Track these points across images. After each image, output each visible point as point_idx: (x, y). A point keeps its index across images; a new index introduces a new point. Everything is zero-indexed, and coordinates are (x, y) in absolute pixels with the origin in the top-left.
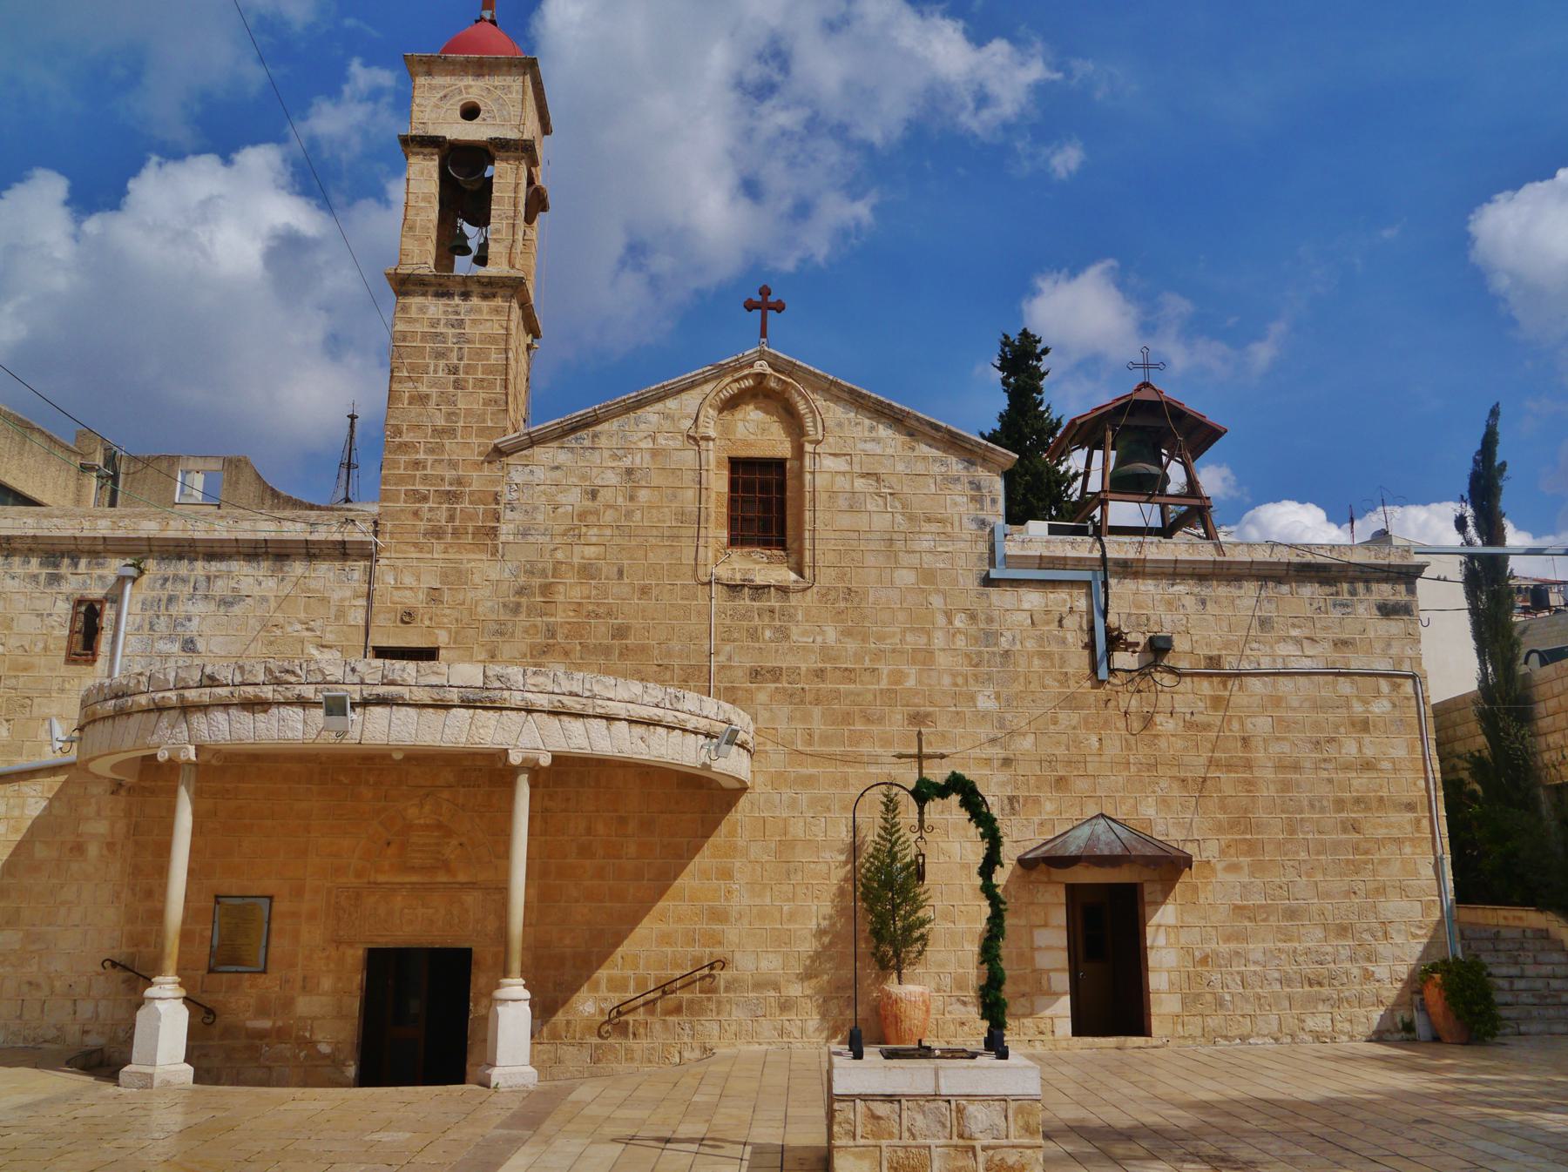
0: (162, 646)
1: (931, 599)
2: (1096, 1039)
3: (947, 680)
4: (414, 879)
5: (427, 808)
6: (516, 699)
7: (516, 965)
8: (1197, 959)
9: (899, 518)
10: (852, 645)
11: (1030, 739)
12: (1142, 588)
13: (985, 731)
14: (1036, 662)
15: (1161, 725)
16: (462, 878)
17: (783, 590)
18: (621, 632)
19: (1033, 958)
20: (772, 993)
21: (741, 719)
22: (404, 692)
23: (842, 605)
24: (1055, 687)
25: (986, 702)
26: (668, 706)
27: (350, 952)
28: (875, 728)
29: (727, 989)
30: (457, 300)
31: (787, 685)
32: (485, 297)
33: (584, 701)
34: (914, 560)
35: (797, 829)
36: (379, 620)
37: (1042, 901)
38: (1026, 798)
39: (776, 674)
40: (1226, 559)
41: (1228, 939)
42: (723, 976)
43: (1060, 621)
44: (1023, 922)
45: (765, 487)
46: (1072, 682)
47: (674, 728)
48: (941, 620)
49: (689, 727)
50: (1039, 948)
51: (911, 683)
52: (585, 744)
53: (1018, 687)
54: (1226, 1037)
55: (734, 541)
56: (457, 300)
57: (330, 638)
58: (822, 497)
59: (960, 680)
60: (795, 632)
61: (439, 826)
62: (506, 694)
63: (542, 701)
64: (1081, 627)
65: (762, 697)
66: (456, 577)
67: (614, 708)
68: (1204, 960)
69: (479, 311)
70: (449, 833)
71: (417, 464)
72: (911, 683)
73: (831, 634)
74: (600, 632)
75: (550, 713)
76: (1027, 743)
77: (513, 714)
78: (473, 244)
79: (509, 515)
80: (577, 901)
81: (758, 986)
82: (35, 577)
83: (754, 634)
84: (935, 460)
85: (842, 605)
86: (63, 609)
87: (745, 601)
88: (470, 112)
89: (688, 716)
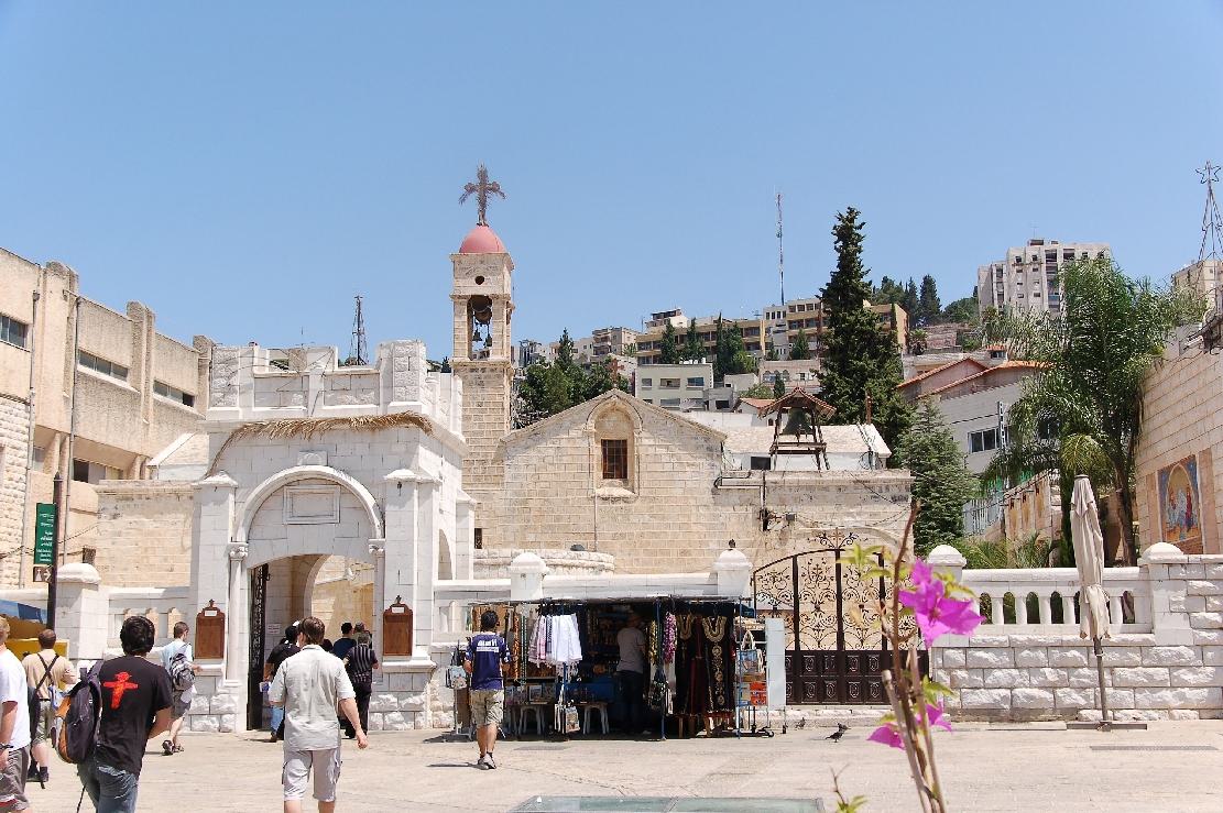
17: (625, 499)
21: (605, 557)
32: (492, 370)
39: (623, 536)
45: (618, 451)
48: (694, 511)
51: (681, 538)
66: (486, 495)
69: (490, 377)
72: (681, 538)
73: (647, 517)
78: (484, 337)
83: (614, 519)
87: (608, 505)
88: (480, 280)
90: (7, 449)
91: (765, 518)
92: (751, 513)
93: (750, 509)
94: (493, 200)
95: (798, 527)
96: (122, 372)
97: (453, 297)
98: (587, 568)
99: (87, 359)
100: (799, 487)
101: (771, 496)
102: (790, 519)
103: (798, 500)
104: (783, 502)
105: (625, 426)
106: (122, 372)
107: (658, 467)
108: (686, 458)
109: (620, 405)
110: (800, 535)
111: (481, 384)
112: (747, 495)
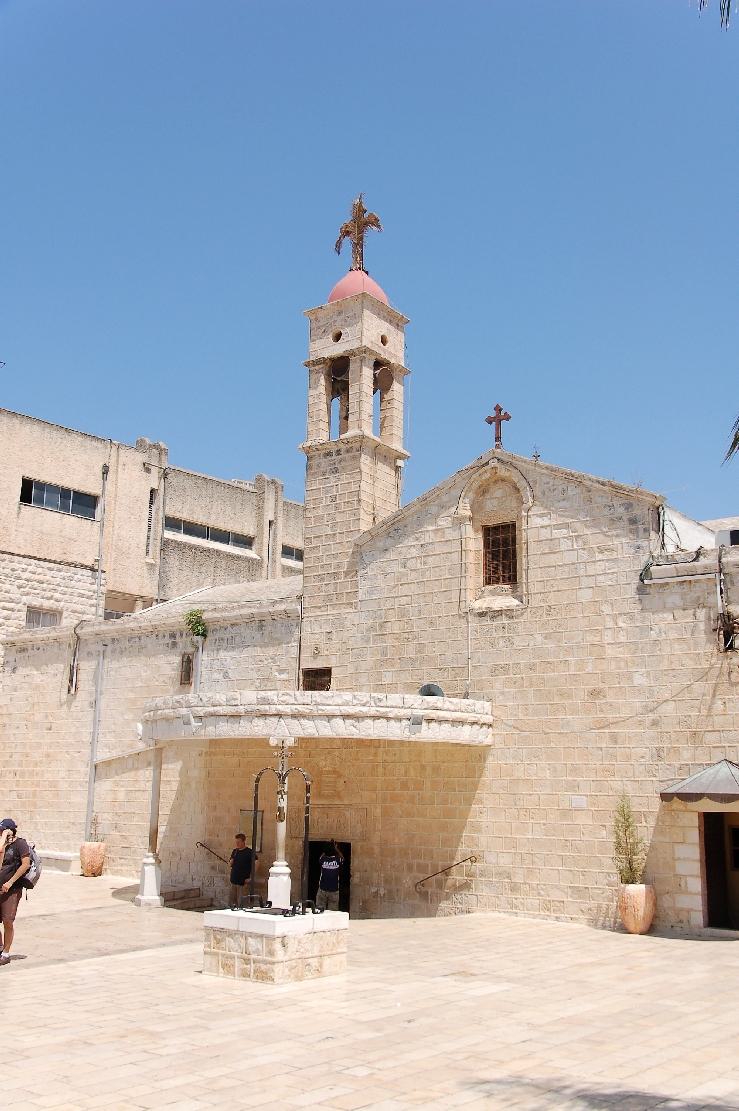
0: (216, 676)
1: (603, 608)
2: (727, 931)
3: (613, 665)
6: (273, 709)
7: (281, 854)
10: (550, 645)
11: (672, 705)
13: (638, 702)
14: (676, 646)
16: (346, 802)
17: (508, 613)
18: (421, 648)
19: (674, 867)
22: (220, 710)
23: (545, 618)
24: (690, 664)
25: (638, 680)
26: (373, 704)
28: (567, 702)
29: (482, 875)
31: (512, 676)
32: (348, 451)
34: (590, 582)
37: (681, 824)
38: (669, 749)
39: (505, 669)
45: (505, 542)
46: (703, 661)
47: (379, 718)
48: (610, 624)
49: (391, 715)
50: (679, 859)
51: (589, 669)
52: (314, 731)
53: (665, 665)
55: (488, 582)
57: (283, 666)
58: (532, 546)
59: (622, 664)
60: (517, 641)
61: (335, 772)
62: (267, 707)
63: (287, 709)
64: (709, 619)
67: (329, 710)
70: (340, 776)
73: (539, 638)
74: (410, 651)
76: (669, 708)
77: (273, 719)
81: (500, 874)
85: (545, 618)
86: (177, 660)
87: (487, 621)
88: (338, 337)
89: (388, 710)
90: (65, 614)
93: (702, 614)
94: (371, 233)
96: (246, 542)
97: (307, 365)
98: (399, 719)
106: (246, 542)
107: (553, 559)
108: (594, 537)
109: (503, 472)
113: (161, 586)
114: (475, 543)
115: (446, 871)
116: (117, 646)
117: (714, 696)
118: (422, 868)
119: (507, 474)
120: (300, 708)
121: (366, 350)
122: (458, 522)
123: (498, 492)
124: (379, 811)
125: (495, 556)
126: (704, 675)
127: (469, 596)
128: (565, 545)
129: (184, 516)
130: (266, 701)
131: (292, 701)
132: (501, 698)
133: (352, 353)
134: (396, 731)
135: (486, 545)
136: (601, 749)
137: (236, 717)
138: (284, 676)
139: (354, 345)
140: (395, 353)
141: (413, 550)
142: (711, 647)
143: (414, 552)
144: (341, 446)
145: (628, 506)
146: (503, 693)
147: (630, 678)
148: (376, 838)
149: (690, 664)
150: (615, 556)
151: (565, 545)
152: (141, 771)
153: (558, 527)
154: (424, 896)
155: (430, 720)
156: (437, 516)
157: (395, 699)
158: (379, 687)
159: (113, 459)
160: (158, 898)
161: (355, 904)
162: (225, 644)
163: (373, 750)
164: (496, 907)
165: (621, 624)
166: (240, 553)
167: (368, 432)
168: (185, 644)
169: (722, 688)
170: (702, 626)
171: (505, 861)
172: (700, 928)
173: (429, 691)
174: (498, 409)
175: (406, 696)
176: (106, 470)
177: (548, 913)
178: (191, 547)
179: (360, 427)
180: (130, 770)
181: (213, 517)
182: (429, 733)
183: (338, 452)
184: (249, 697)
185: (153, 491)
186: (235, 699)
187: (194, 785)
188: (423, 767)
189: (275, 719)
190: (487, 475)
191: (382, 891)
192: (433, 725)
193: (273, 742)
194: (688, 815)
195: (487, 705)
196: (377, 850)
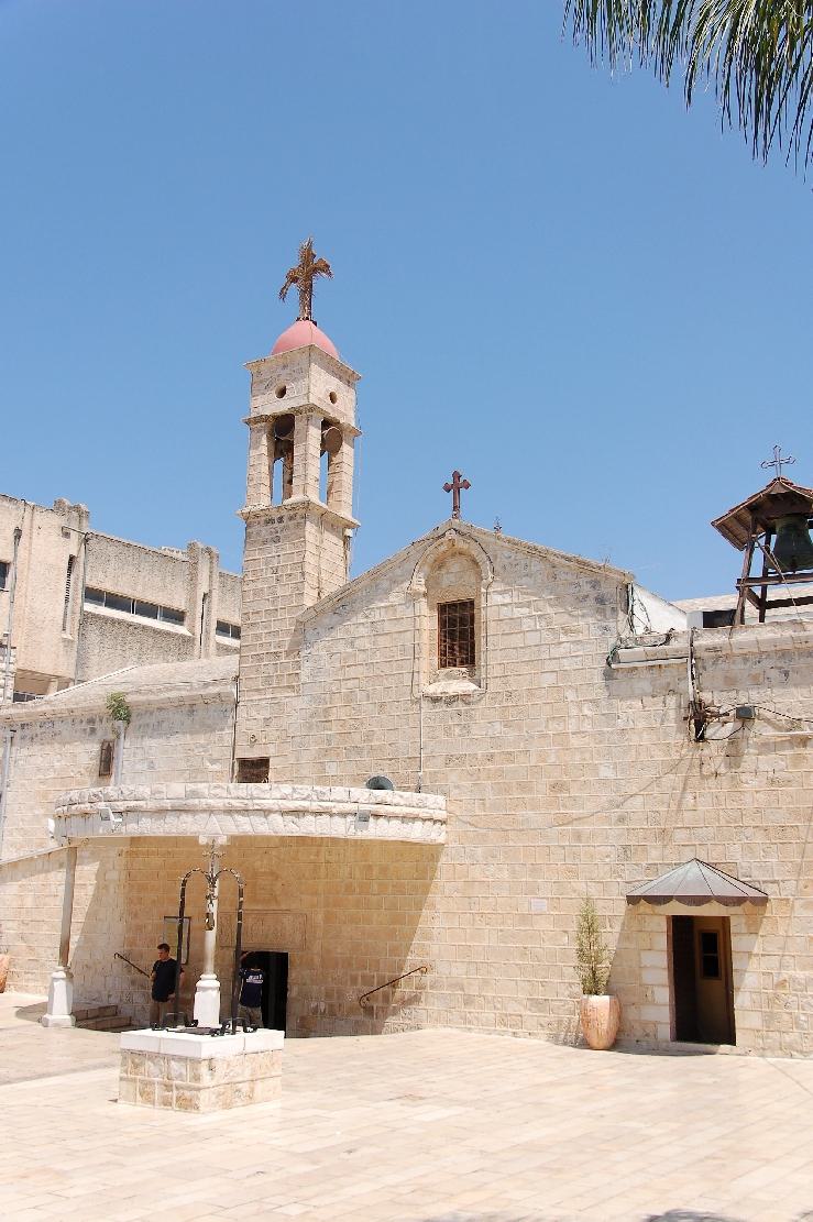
0: (139, 767)
1: (567, 694)
3: (577, 757)
4: (260, 907)
5: (265, 862)
7: (210, 965)
8: (775, 981)
9: (544, 633)
10: (512, 734)
12: (732, 666)
14: (645, 735)
15: (747, 783)
17: (464, 698)
18: (369, 736)
19: (640, 975)
20: (460, 992)
24: (659, 756)
26: (315, 798)
27: (228, 953)
29: (432, 987)
30: (276, 525)
32: (291, 518)
33: (246, 801)
34: (552, 666)
35: (476, 873)
36: (242, 741)
40: (807, 633)
41: (804, 968)
42: (428, 978)
43: (664, 702)
44: (633, 946)
46: (673, 752)
47: (321, 814)
48: (574, 711)
49: (334, 811)
50: (645, 967)
51: (552, 759)
54: (801, 1052)
55: (443, 665)
56: (276, 525)
57: (215, 756)
59: (587, 756)
60: (475, 730)
61: (272, 873)
62: (196, 801)
64: (680, 707)
65: (453, 777)
67: (268, 804)
68: (782, 984)
71: (257, 637)
75: (225, 811)
79: (307, 664)
80: (345, 923)
82: (85, 730)
84: (571, 584)
86: (96, 748)
87: (441, 708)
88: (282, 393)
91: (699, 717)
92: (672, 709)
93: (672, 701)
94: (320, 281)
95: (761, 731)
96: (177, 616)
97: (248, 422)
98: (344, 815)
99: (93, 595)
100: (761, 656)
101: (710, 675)
102: (745, 715)
103: (757, 681)
104: (731, 683)
105: (471, 578)
106: (177, 616)
107: (517, 640)
108: (560, 619)
109: (461, 545)
110: (767, 747)
111: (275, 541)
112: (667, 677)
113: (81, 663)
114: (429, 623)
115: (394, 983)
116: (27, 732)
117: (684, 789)
118: (367, 980)
119: (466, 546)
120: (234, 802)
121: (312, 408)
122: (412, 598)
123: (455, 566)
124: (320, 918)
125: (451, 635)
126: (673, 768)
127: (423, 678)
128: (527, 624)
129: (108, 586)
130: (195, 794)
131: (225, 795)
132: (457, 791)
133: (298, 411)
134: (339, 828)
135: (442, 623)
136: (564, 847)
137: (161, 812)
138: (216, 767)
139: (303, 402)
140: (346, 411)
141: (361, 629)
142: (682, 736)
143: (363, 631)
144: (284, 513)
145: (595, 585)
146: (458, 787)
147: (595, 768)
148: (316, 948)
149: (659, 756)
150: (581, 637)
151: (527, 624)
152: (53, 874)
153: (519, 605)
154: (369, 1011)
155: (377, 816)
156: (387, 592)
157: (339, 792)
158: (323, 779)
159: (27, 521)
160: (69, 1017)
161: (291, 1022)
162: (150, 731)
163: (314, 849)
164: (448, 1023)
165: (586, 712)
166: (116, 616)
167: (314, 497)
168: (104, 730)
169: (694, 781)
170: (672, 714)
171: (458, 971)
172: (667, 1041)
173: (377, 784)
174: (457, 476)
175: (352, 789)
176: (18, 534)
177: (505, 1029)
178: (113, 621)
179: (304, 492)
180: (40, 872)
181: (140, 588)
182: (377, 830)
183: (281, 520)
184: (177, 789)
185: (72, 559)
186: (160, 792)
187: (112, 890)
188: (370, 867)
189: (205, 815)
190: (443, 548)
191: (322, 1007)
192: (381, 820)
193: (203, 840)
194: (656, 919)
195: (441, 799)
196: (317, 960)
